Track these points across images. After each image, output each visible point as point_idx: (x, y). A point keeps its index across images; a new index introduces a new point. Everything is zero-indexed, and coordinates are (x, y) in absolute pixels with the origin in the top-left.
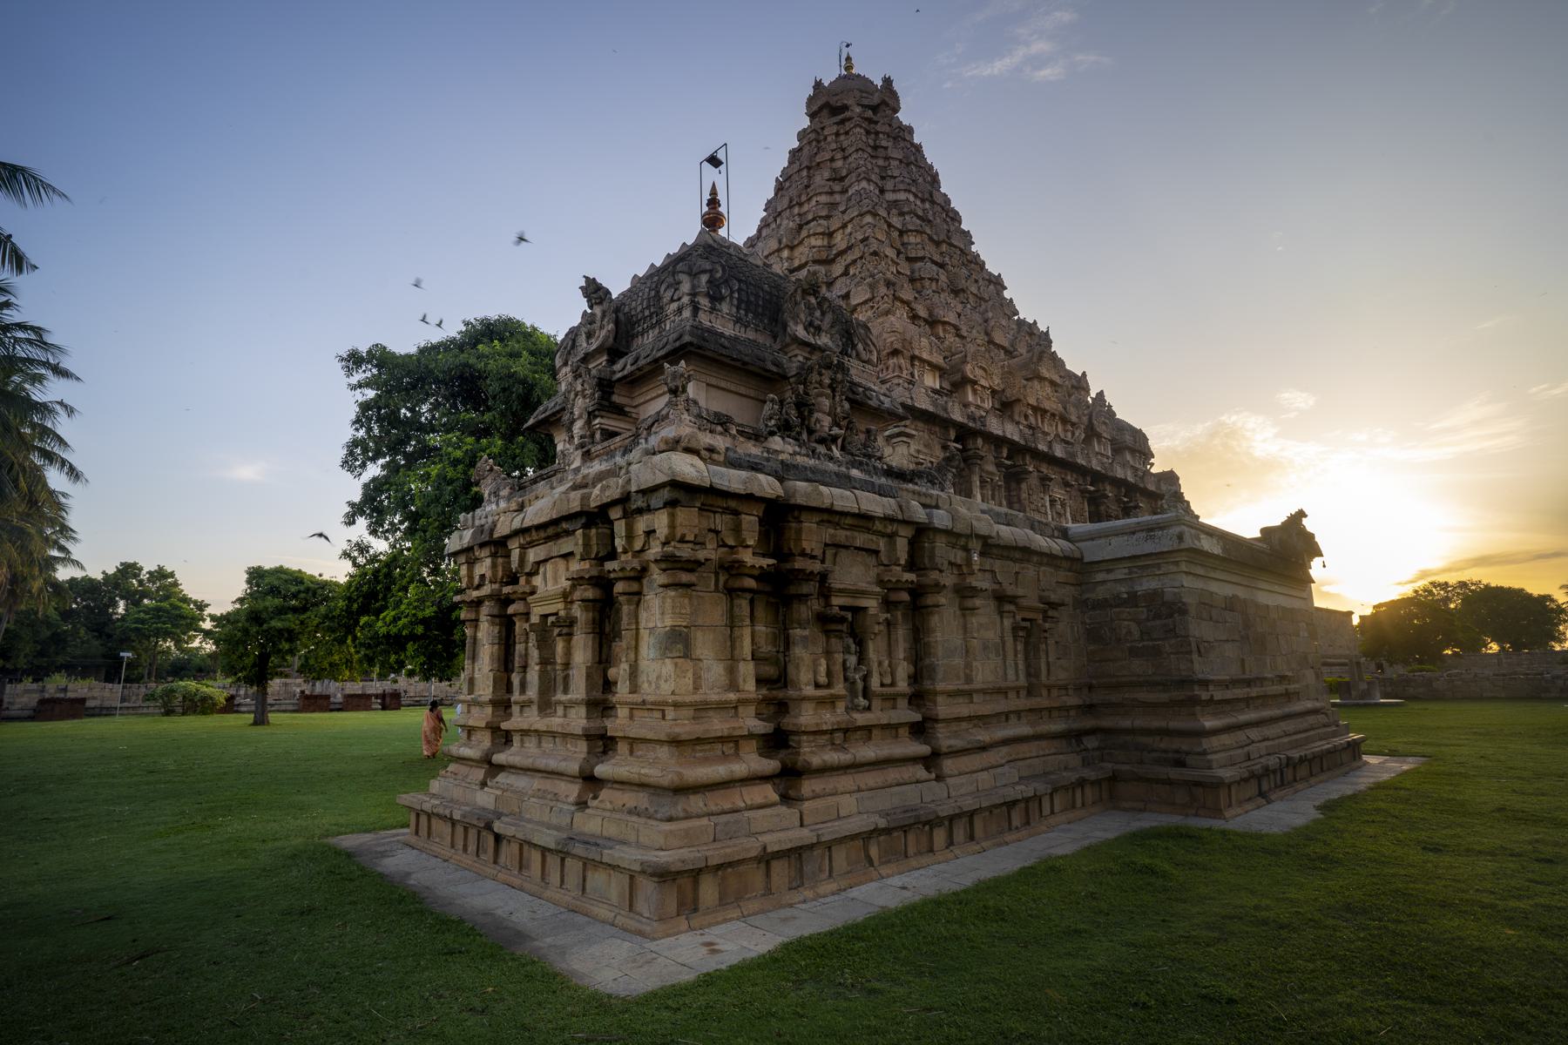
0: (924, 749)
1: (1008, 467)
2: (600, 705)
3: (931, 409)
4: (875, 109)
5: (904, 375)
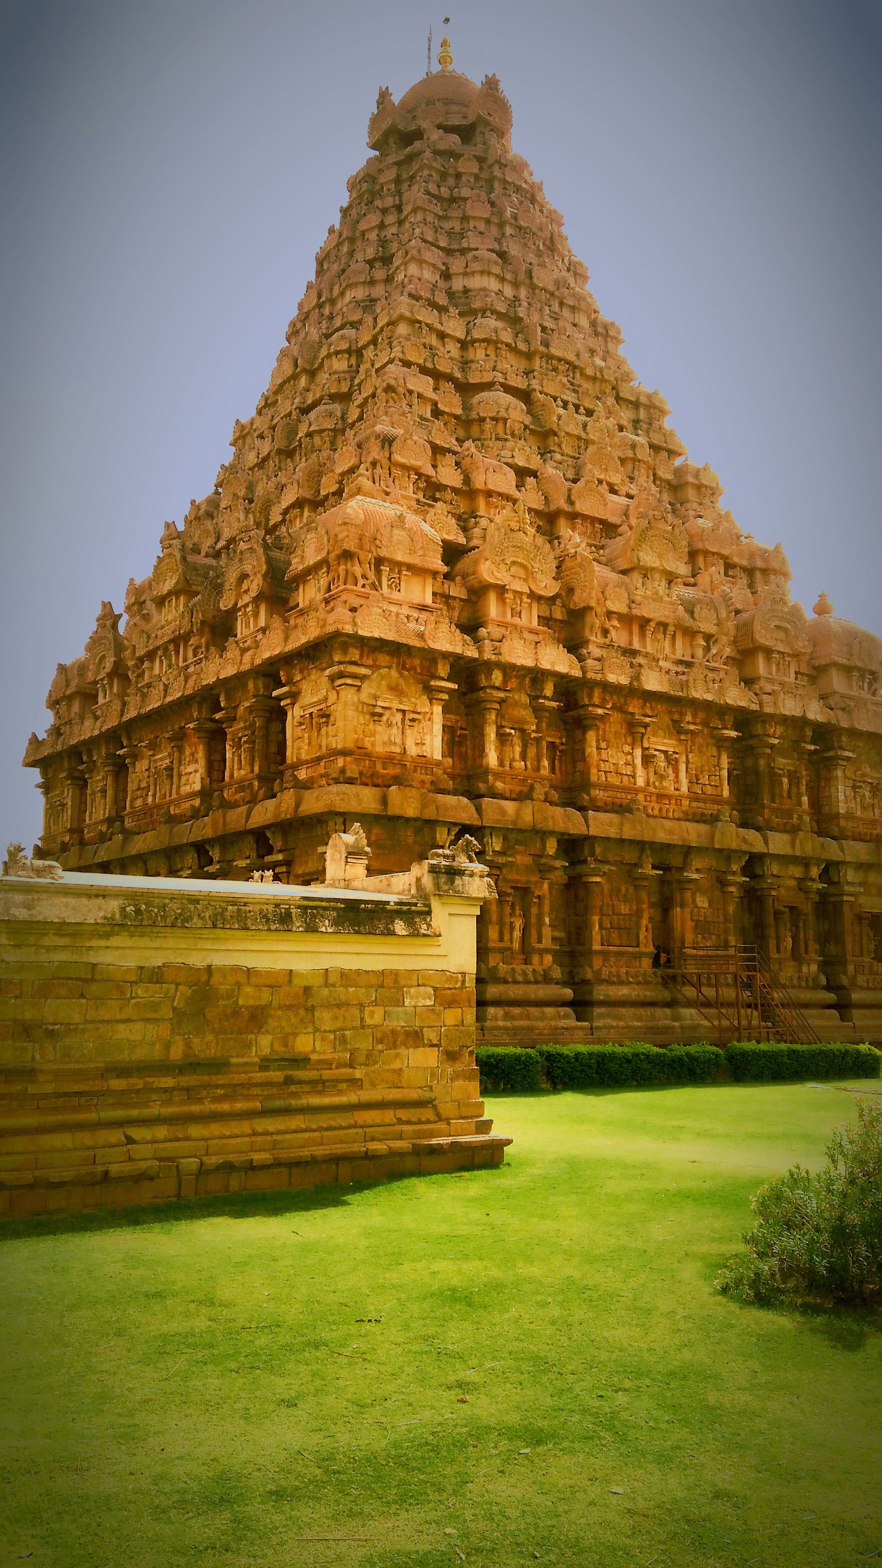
4: (466, 133)
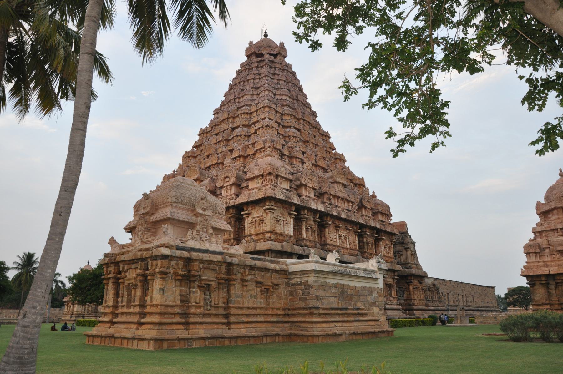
0: (226, 321)
1: (319, 222)
2: (143, 305)
3: (284, 198)
4: (275, 56)
5: (273, 183)
